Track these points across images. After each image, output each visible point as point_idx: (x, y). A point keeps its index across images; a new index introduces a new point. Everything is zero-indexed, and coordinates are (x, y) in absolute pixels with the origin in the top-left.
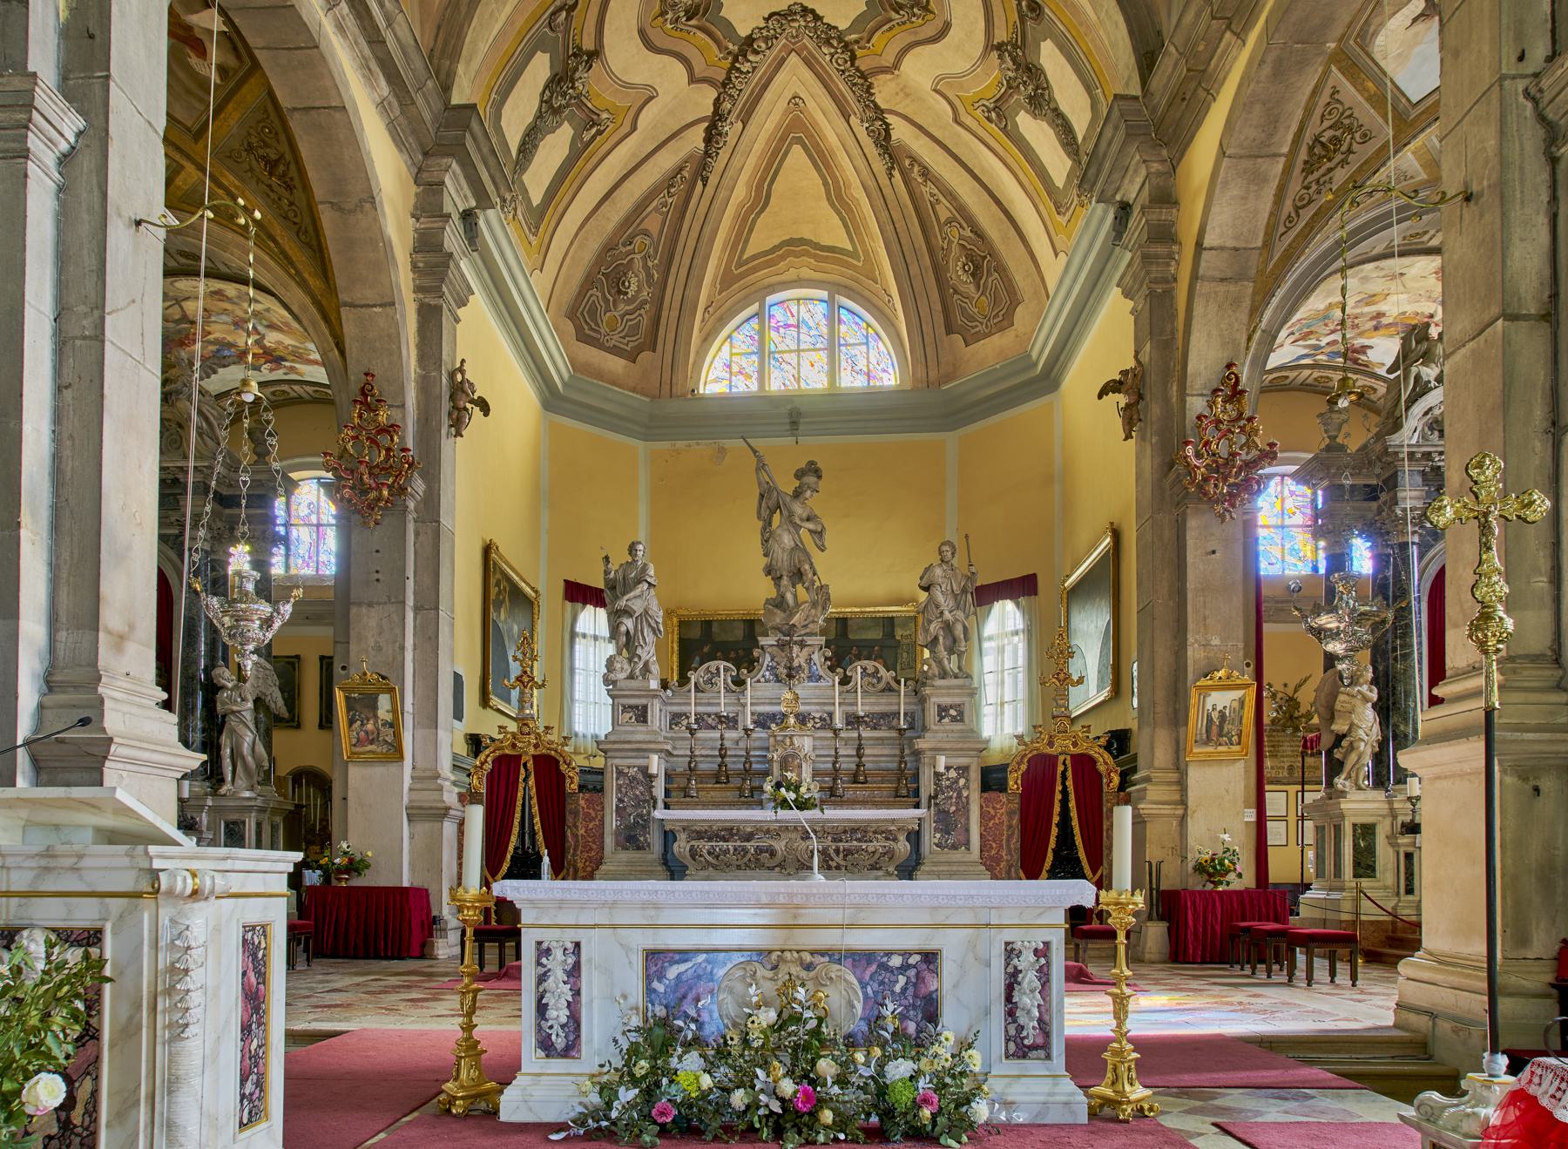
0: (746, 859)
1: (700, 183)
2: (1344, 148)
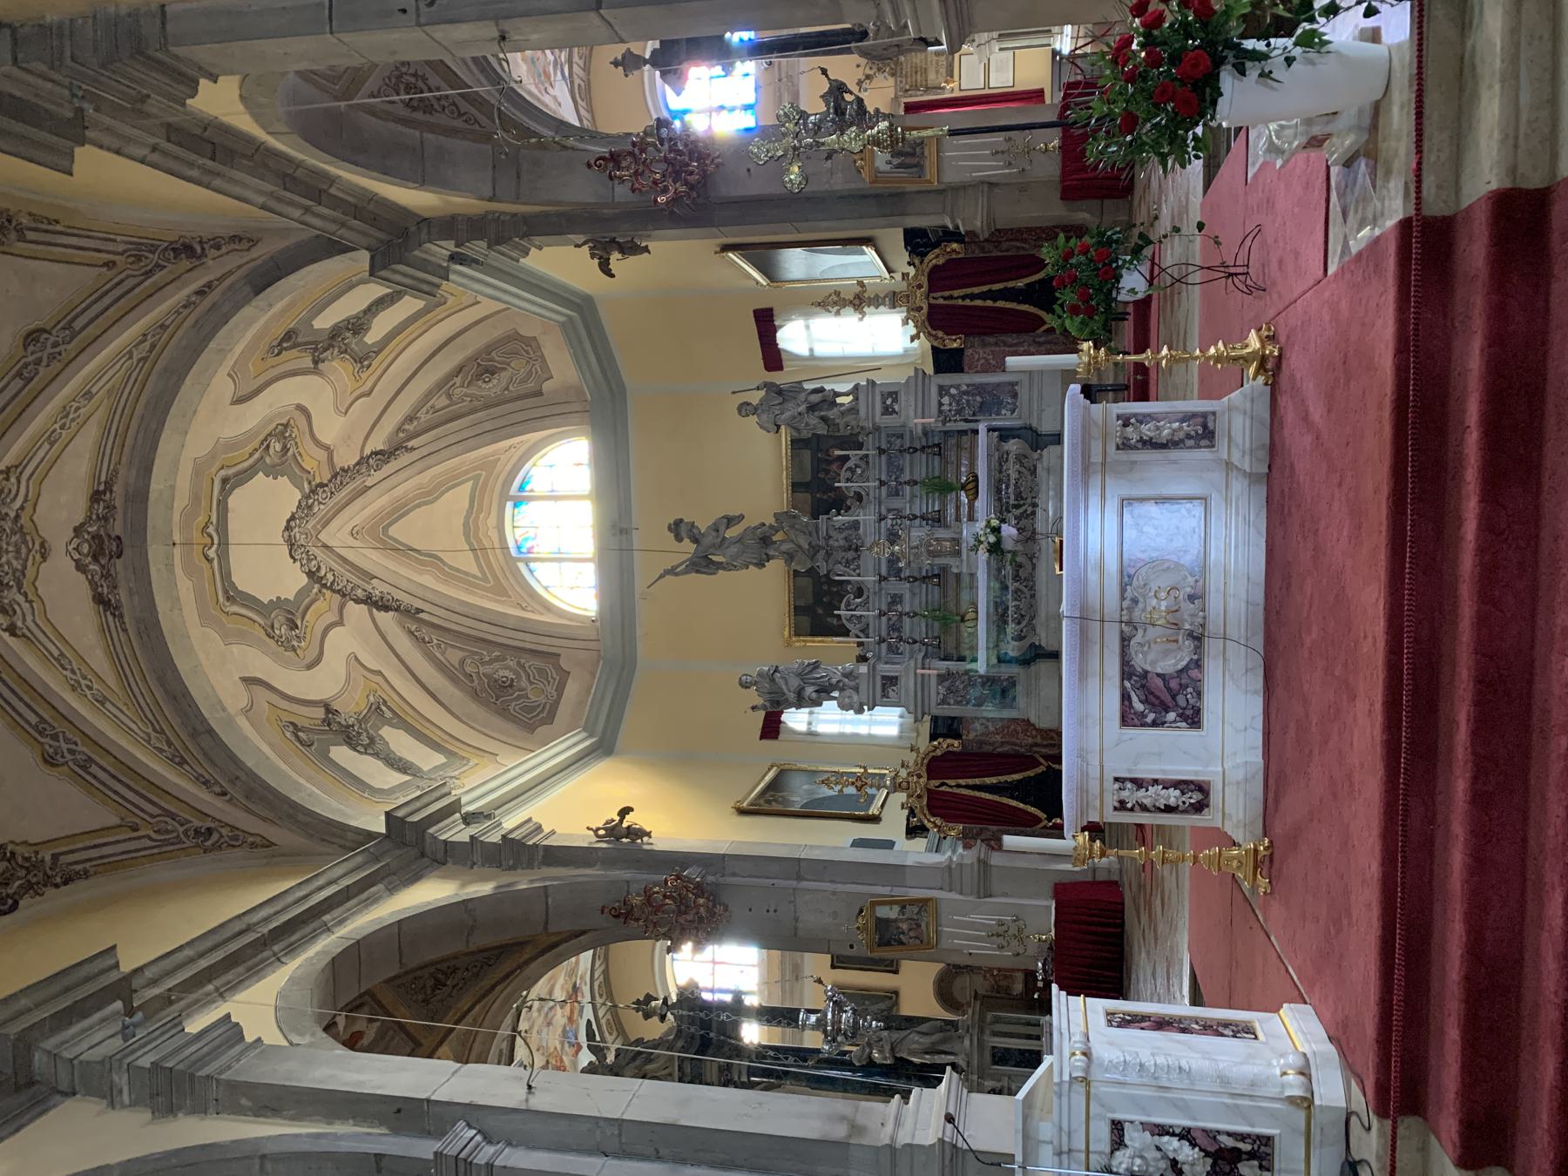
0: (1025, 590)
1: (422, 615)
2: (413, 80)
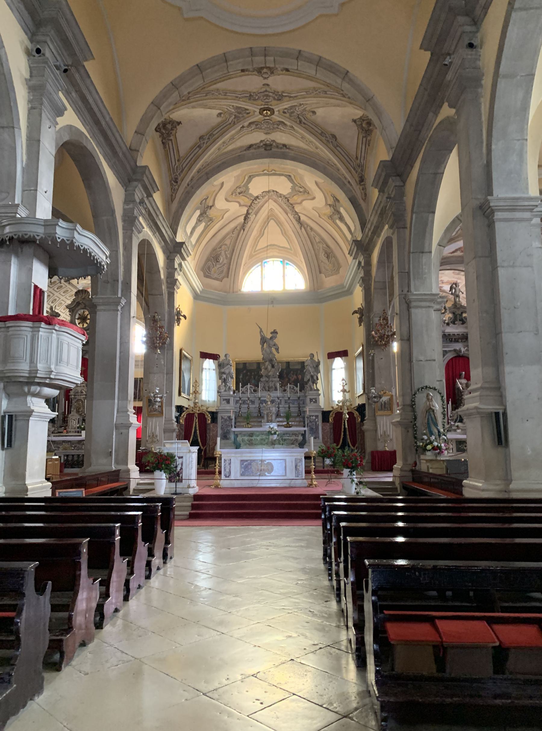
1: (242, 230)
